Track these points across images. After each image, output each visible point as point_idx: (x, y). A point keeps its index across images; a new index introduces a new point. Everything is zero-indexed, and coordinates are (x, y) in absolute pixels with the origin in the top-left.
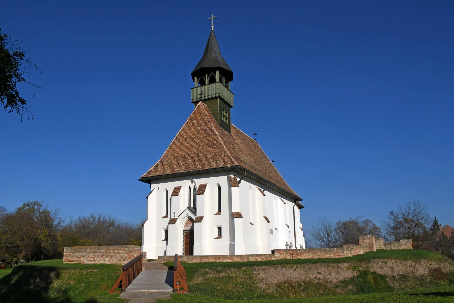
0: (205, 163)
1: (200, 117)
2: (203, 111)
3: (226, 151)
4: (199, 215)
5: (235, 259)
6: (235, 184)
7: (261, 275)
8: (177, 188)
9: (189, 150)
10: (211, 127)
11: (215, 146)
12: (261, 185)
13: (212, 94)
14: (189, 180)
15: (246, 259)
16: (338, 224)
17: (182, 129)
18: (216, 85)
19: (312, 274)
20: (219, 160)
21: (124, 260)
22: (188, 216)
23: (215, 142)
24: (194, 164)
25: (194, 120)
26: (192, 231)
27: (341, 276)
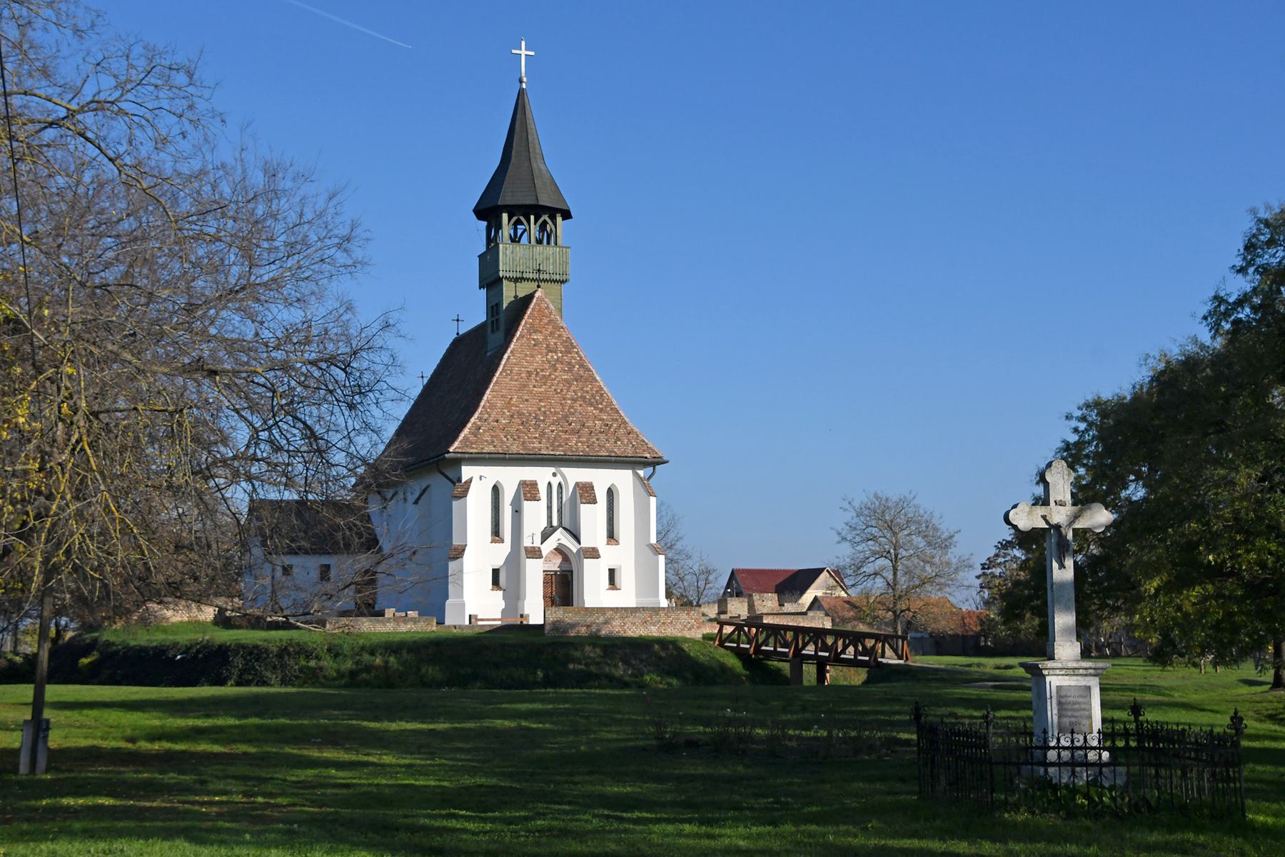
0: (592, 440)
4: (586, 542)
9: (543, 404)
11: (600, 406)
21: (690, 629)
23: (598, 398)
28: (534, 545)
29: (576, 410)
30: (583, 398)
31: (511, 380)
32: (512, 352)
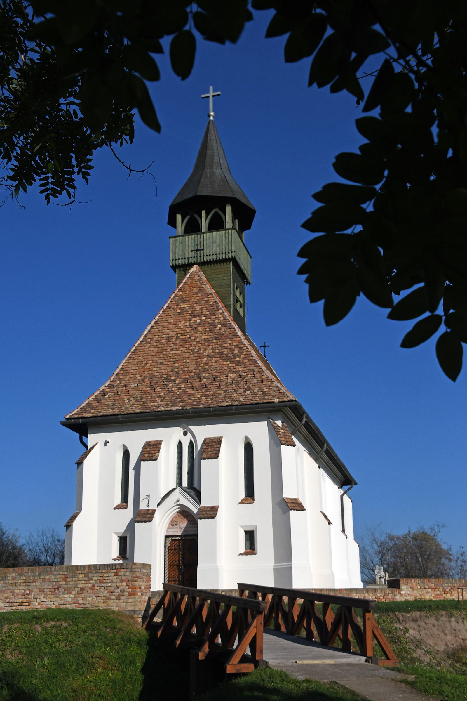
0: (219, 392)
1: (197, 298)
2: (203, 286)
3: (263, 371)
4: (206, 502)
6: (288, 440)
7: (411, 632)
8: (150, 443)
9: (177, 365)
10: (224, 319)
11: (237, 359)
13: (217, 253)
14: (179, 428)
17: (158, 319)
18: (227, 235)
20: (249, 388)
21: (118, 598)
22: (180, 505)
23: (236, 352)
24: (193, 395)
25: (183, 302)
26: (194, 537)
28: (150, 508)
29: (210, 367)
30: (221, 354)
31: (150, 347)
32: (156, 323)
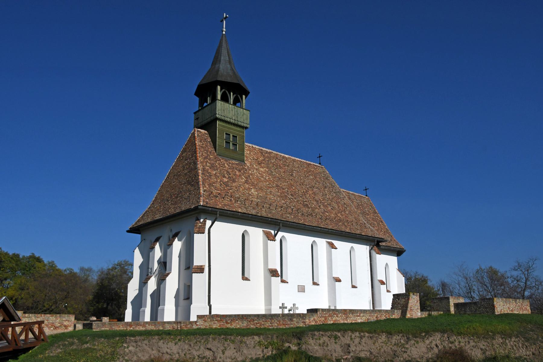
5: (149, 326)
12: (275, 226)
15: (161, 326)
16: (477, 272)
19: (197, 350)
27: (242, 354)
